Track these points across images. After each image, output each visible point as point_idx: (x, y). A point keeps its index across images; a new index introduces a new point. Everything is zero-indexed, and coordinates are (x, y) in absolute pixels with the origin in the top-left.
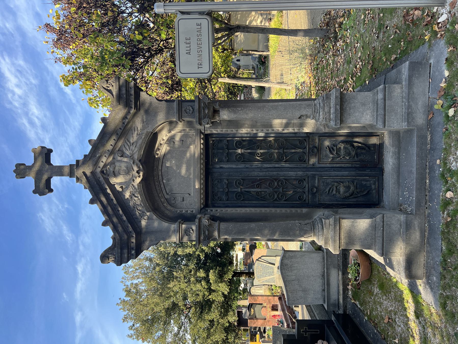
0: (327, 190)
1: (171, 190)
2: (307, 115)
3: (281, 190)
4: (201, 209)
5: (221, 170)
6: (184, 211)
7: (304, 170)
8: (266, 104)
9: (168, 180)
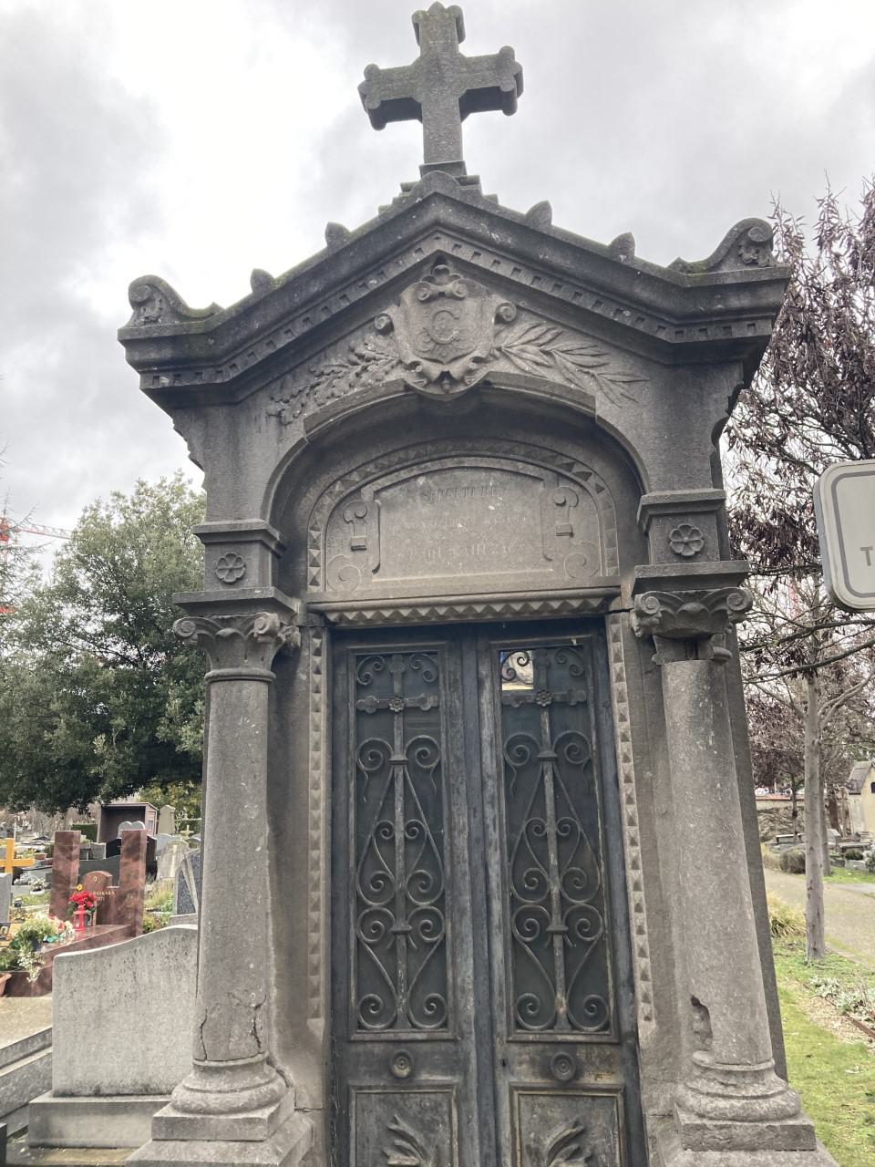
0: (404, 1126)
1: (391, 506)
2: (709, 1034)
3: (401, 925)
4: (322, 614)
5: (470, 682)
6: (315, 553)
7: (484, 1022)
8: (744, 852)
9: (426, 493)
